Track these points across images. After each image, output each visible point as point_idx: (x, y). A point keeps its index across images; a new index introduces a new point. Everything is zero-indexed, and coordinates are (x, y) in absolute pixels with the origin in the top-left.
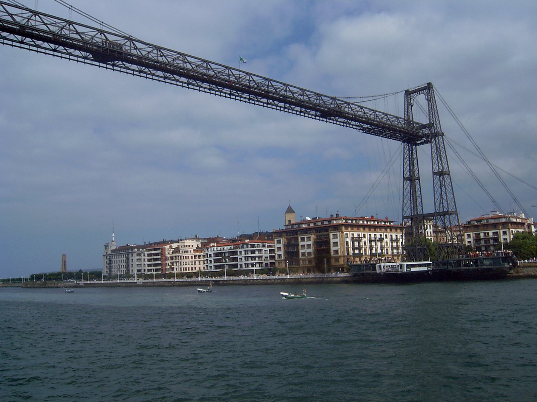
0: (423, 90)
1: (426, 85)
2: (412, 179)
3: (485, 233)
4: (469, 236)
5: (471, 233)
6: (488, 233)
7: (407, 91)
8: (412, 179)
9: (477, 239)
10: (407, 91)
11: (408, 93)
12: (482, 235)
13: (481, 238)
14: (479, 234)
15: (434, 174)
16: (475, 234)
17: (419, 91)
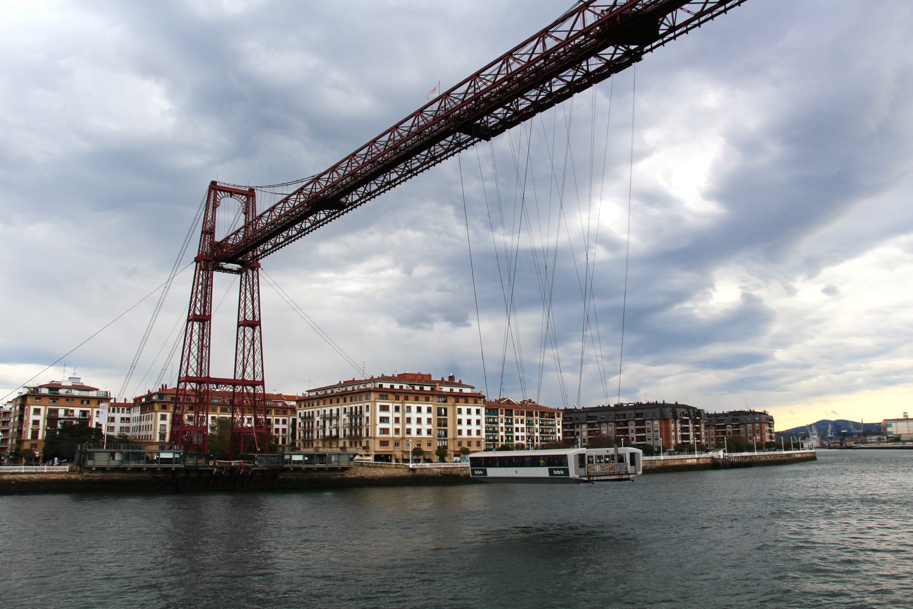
0: (224, 191)
1: (247, 189)
2: (201, 317)
3: (66, 411)
4: (37, 412)
5: (42, 408)
6: (72, 411)
7: (214, 183)
8: (201, 317)
9: (52, 419)
10: (214, 183)
11: (214, 187)
12: (61, 413)
13: (60, 416)
14: (56, 411)
15: (259, 323)
16: (50, 410)
17: (232, 192)
